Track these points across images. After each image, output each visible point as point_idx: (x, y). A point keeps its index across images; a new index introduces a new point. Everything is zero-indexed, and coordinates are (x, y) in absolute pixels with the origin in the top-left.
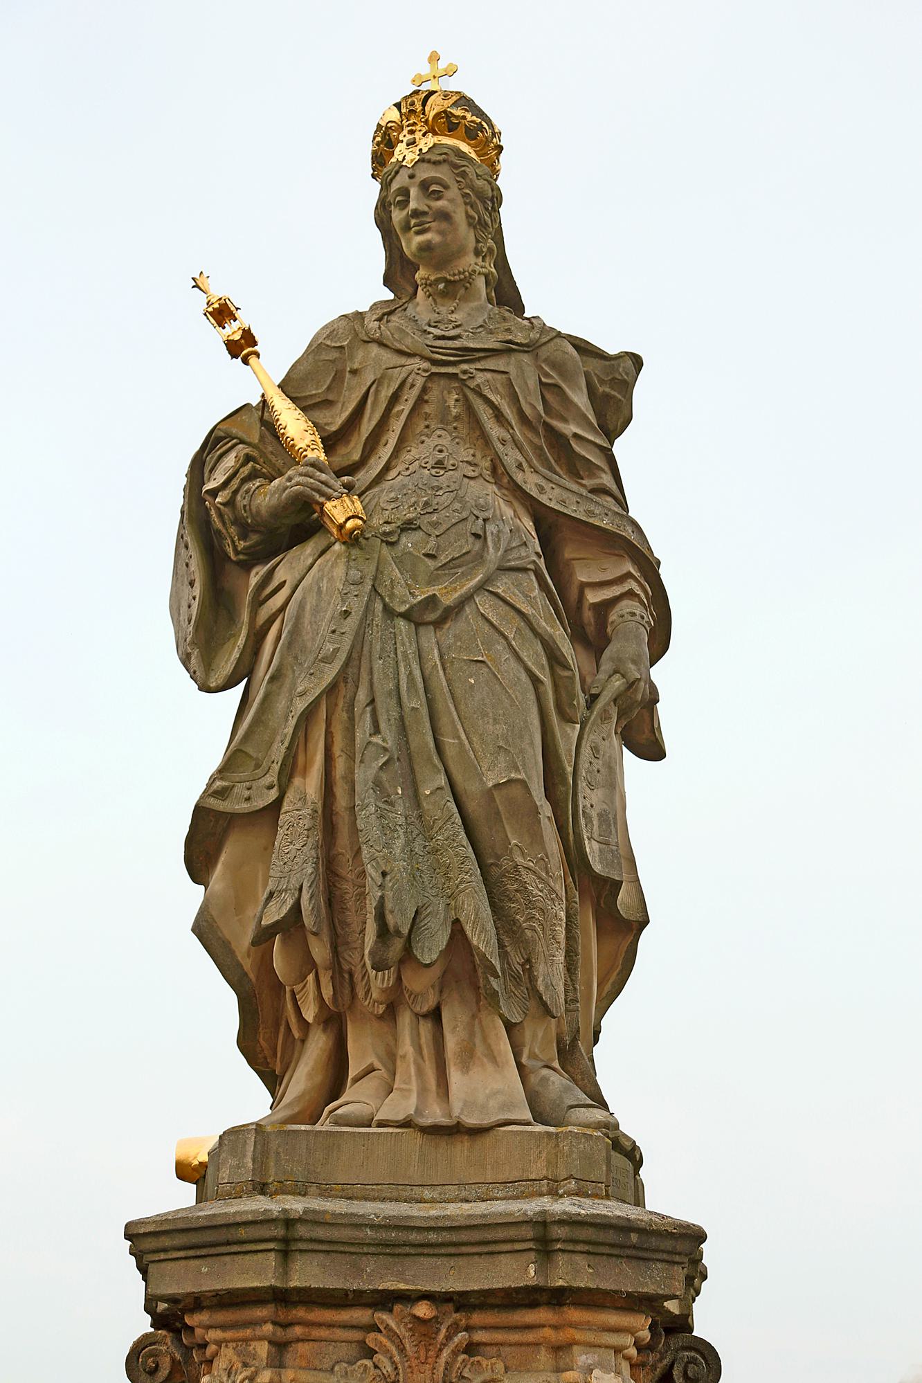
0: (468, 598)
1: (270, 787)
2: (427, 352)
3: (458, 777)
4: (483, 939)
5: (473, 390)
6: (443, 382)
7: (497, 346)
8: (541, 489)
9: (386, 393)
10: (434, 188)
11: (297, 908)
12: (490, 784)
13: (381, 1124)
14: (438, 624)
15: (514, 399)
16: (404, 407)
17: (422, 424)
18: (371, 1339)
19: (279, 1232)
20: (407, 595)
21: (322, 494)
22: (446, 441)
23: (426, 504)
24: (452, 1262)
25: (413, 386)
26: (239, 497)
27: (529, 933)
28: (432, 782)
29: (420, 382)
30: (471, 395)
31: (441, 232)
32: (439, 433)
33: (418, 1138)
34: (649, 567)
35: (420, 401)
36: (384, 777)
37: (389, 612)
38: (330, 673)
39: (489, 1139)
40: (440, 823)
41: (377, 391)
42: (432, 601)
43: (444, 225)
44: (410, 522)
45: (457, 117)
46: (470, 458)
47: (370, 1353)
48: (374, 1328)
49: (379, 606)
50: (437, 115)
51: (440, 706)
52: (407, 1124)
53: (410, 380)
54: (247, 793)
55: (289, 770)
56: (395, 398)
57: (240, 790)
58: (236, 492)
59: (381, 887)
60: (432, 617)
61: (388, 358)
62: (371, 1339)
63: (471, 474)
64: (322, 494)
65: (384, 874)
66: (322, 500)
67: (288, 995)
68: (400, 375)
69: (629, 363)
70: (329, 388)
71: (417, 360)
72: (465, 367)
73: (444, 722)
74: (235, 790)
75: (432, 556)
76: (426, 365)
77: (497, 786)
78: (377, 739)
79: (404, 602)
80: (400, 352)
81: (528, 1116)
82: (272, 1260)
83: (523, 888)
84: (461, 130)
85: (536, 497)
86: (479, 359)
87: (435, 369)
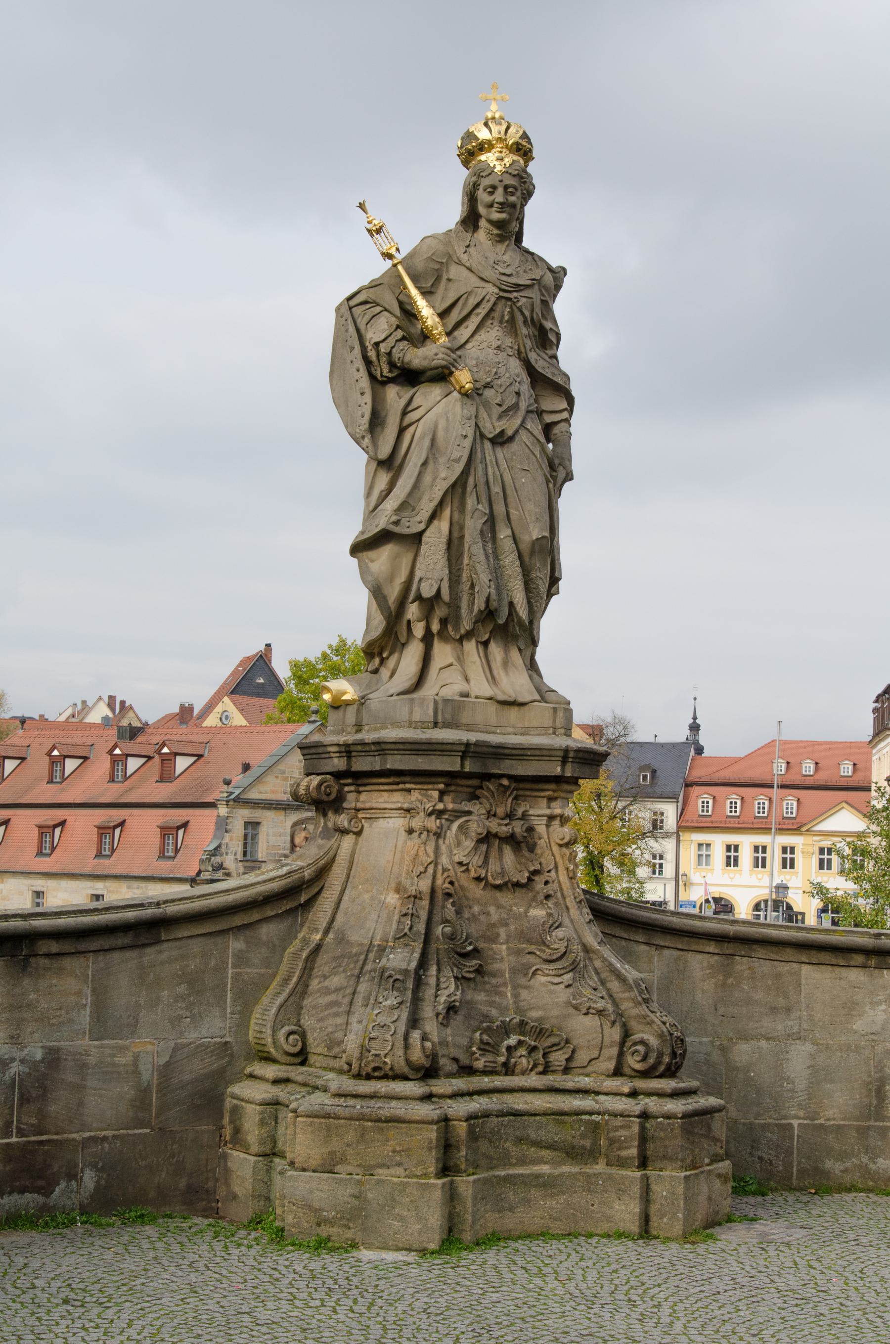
0: (516, 432)
1: (420, 522)
2: (498, 283)
3: (517, 532)
4: (522, 612)
5: (518, 308)
6: (503, 301)
7: (529, 282)
8: (536, 360)
9: (472, 301)
10: (510, 190)
11: (439, 591)
12: (534, 538)
13: (476, 697)
14: (502, 444)
15: (532, 311)
16: (482, 311)
17: (490, 321)
18: (478, 792)
19: (462, 748)
20: (491, 427)
21: (454, 366)
22: (500, 334)
23: (496, 373)
24: (519, 762)
25: (488, 301)
26: (394, 350)
27: (535, 608)
28: (504, 533)
29: (493, 300)
30: (516, 310)
31: (510, 214)
32: (497, 328)
33: (495, 705)
34: (570, 400)
35: (492, 310)
36: (485, 528)
37: (482, 436)
38: (459, 468)
39: (526, 708)
40: (507, 554)
41: (467, 298)
42: (502, 432)
43: (512, 210)
44: (489, 383)
45: (522, 146)
46: (510, 345)
47: (477, 798)
48: (481, 787)
49: (478, 434)
50: (513, 144)
51: (508, 492)
52: (491, 699)
53: (487, 298)
54: (408, 524)
55: (433, 516)
56: (477, 306)
57: (404, 521)
58: (393, 347)
59: (489, 587)
60: (500, 440)
61: (474, 281)
62: (478, 792)
63: (511, 354)
64: (454, 366)
65: (490, 580)
66: (453, 369)
67: (405, 623)
68: (481, 293)
69: (562, 272)
70: (432, 285)
71: (490, 285)
72: (515, 294)
73: (510, 500)
74: (402, 522)
75: (500, 405)
76: (496, 290)
77: (537, 539)
78: (480, 507)
79: (491, 433)
80: (482, 279)
81: (539, 698)
82: (458, 760)
83: (537, 588)
84: (522, 152)
85: (551, 377)
86: (521, 290)
87: (502, 294)
